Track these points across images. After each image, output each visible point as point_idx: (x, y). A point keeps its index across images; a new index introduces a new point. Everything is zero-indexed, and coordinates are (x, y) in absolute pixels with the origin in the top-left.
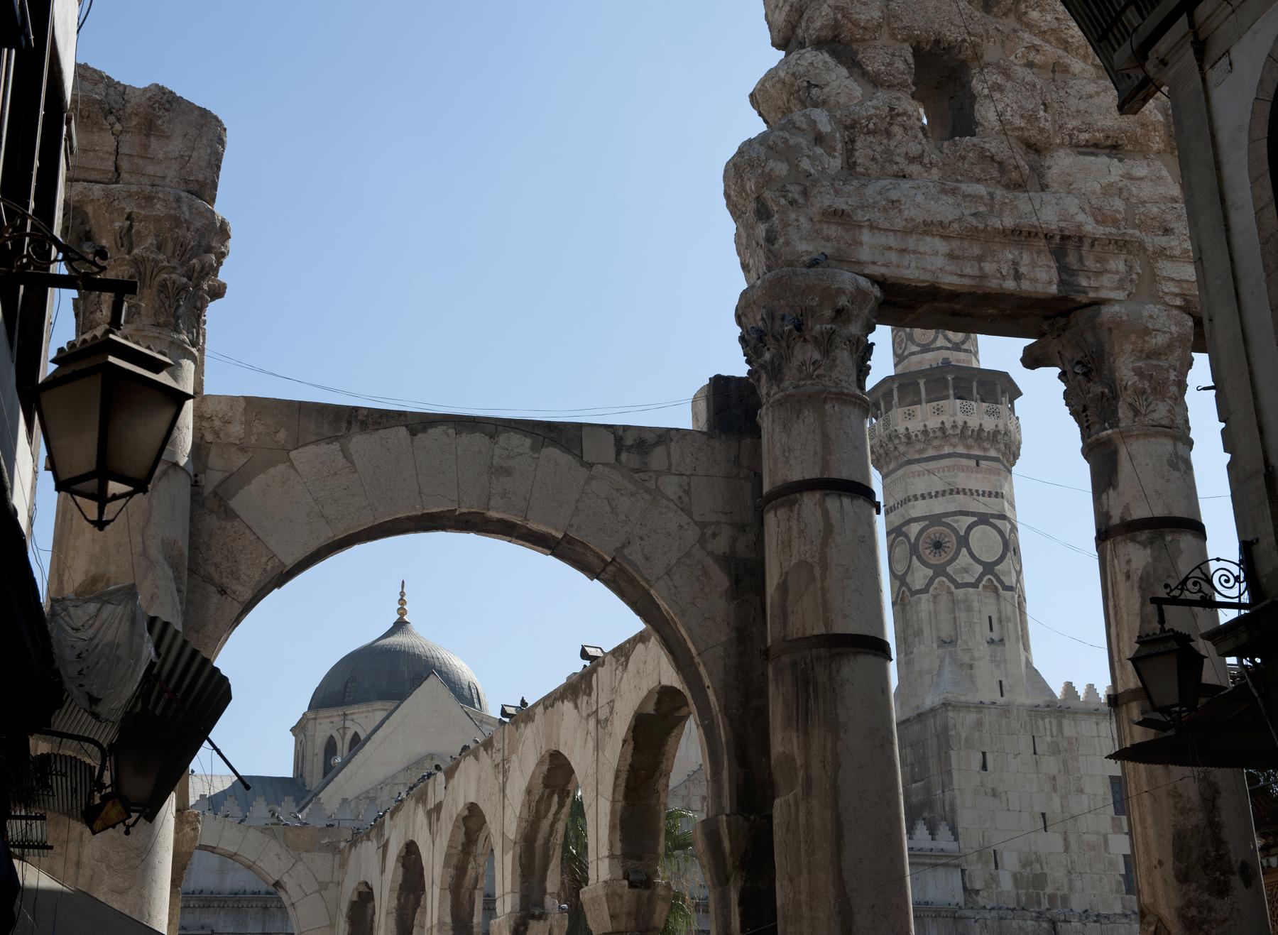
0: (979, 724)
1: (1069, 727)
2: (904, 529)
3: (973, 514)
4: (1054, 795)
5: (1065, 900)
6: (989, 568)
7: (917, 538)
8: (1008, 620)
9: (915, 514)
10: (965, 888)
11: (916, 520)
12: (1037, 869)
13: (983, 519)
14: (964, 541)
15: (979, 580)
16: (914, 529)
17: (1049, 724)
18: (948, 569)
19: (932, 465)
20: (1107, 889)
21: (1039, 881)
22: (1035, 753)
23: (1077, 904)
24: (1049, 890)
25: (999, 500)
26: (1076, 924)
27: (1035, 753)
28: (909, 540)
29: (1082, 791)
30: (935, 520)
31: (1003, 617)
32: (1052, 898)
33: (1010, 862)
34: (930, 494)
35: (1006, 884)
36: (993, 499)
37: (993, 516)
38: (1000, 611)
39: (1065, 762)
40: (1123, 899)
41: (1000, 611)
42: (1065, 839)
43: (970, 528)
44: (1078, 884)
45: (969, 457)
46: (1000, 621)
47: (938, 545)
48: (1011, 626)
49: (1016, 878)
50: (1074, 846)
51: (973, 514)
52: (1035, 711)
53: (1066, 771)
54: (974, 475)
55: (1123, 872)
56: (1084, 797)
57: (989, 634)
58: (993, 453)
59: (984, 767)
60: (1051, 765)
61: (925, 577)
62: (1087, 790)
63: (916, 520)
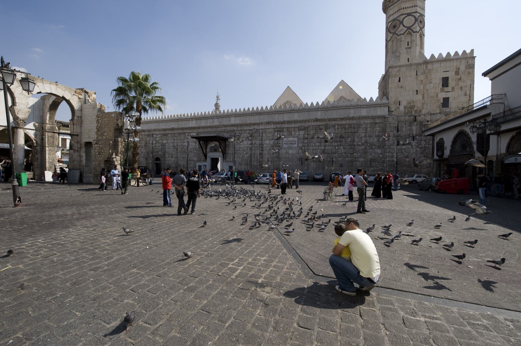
0: (400, 70)
1: (430, 66)
5: (420, 111)
8: (414, 41)
10: (389, 111)
12: (412, 104)
21: (412, 107)
23: (423, 112)
24: (415, 109)
26: (423, 116)
29: (431, 83)
32: (416, 111)
33: (404, 103)
35: (402, 108)
39: (427, 76)
44: (425, 107)
49: (405, 107)
52: (419, 64)
53: (427, 78)
55: (442, 102)
56: (432, 85)
57: (407, 46)
59: (399, 81)
60: (421, 77)
62: (434, 82)
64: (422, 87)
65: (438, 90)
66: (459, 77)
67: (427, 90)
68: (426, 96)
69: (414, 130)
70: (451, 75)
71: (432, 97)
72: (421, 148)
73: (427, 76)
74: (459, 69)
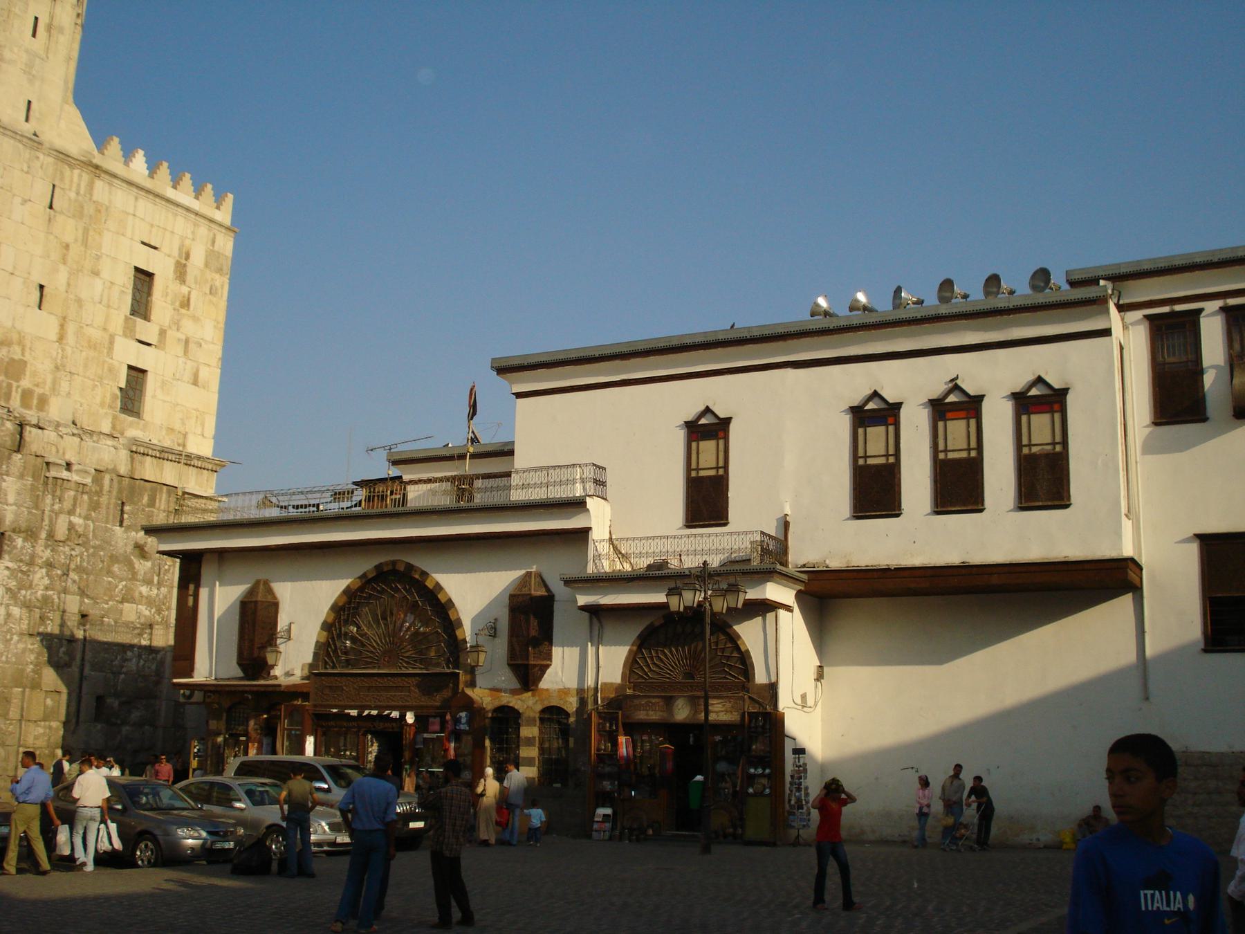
4: (62, 267)
17: (78, 177)
20: (98, 400)
22: (51, 207)
26: (50, 435)
27: (51, 207)
29: (96, 273)
31: (55, 23)
38: (52, 17)
40: (115, 418)
41: (52, 17)
42: (62, 326)
44: (64, 386)
46: (49, 28)
48: (62, 39)
50: (70, 338)
53: (85, 243)
55: (123, 385)
60: (68, 229)
62: (105, 274)
64: (62, 276)
66: (185, 290)
67: (79, 301)
68: (71, 328)
69: (11, 498)
70: (161, 266)
71: (92, 346)
72: (27, 606)
73: (86, 231)
74: (187, 257)
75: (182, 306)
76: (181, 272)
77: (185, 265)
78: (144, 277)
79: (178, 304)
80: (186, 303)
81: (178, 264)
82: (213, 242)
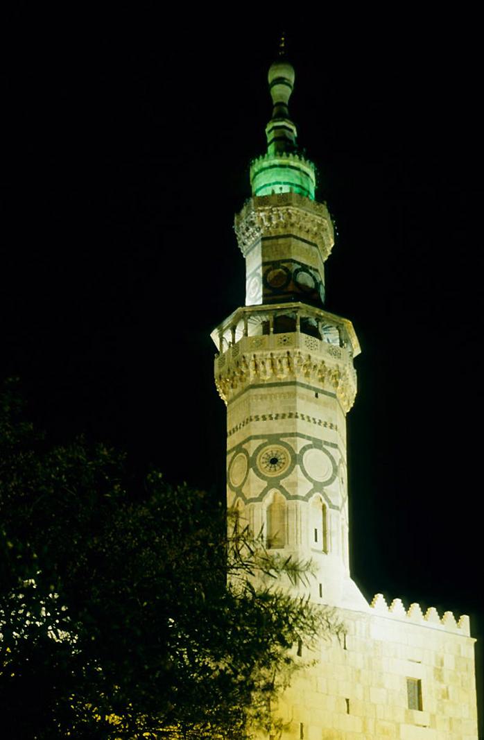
2: (244, 446)
3: (309, 438)
6: (318, 487)
7: (256, 454)
9: (254, 433)
11: (257, 437)
13: (317, 444)
14: (296, 459)
15: (309, 495)
16: (254, 444)
18: (282, 482)
19: (274, 390)
25: (333, 431)
28: (247, 455)
30: (274, 439)
34: (270, 416)
36: (328, 428)
37: (326, 443)
43: (304, 449)
45: (309, 387)
47: (274, 461)
51: (309, 438)
54: (312, 405)
58: (331, 389)
61: (259, 487)
63: (257, 437)
65: (401, 716)
66: (444, 686)
74: (442, 664)
75: (443, 697)
76: (439, 675)
77: (441, 670)
78: (416, 689)
79: (440, 697)
80: (446, 695)
81: (436, 669)
82: (460, 651)
